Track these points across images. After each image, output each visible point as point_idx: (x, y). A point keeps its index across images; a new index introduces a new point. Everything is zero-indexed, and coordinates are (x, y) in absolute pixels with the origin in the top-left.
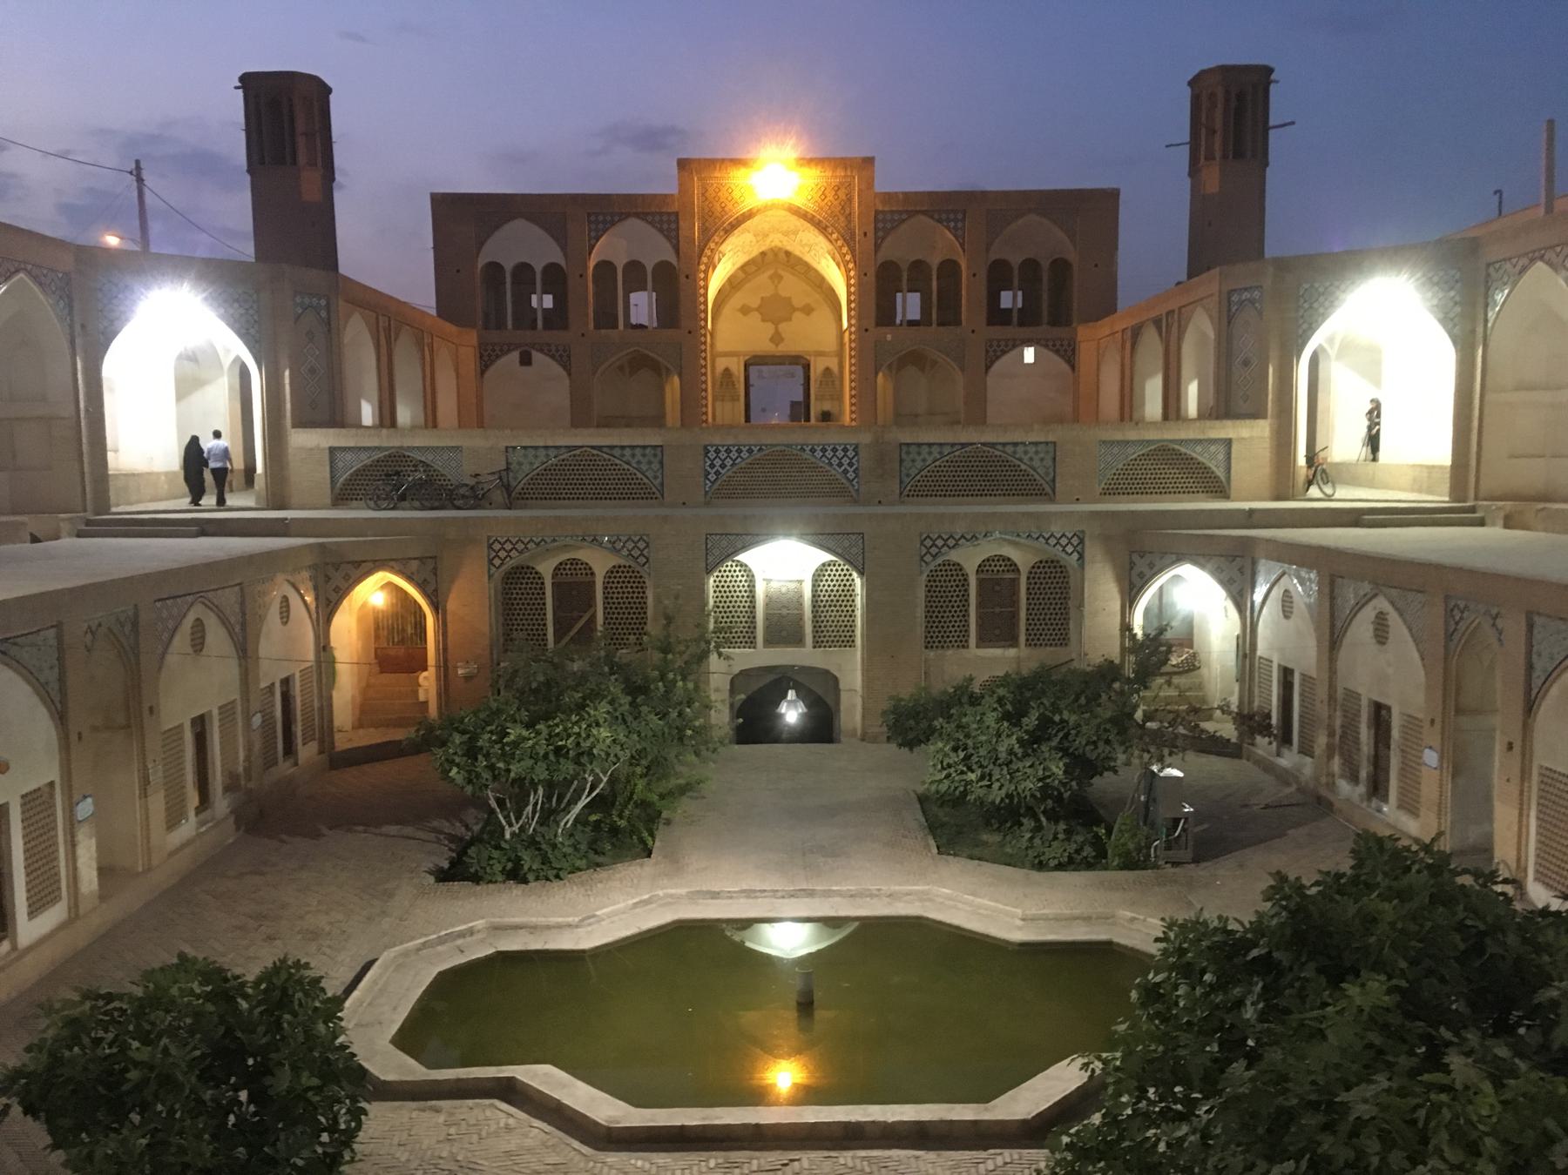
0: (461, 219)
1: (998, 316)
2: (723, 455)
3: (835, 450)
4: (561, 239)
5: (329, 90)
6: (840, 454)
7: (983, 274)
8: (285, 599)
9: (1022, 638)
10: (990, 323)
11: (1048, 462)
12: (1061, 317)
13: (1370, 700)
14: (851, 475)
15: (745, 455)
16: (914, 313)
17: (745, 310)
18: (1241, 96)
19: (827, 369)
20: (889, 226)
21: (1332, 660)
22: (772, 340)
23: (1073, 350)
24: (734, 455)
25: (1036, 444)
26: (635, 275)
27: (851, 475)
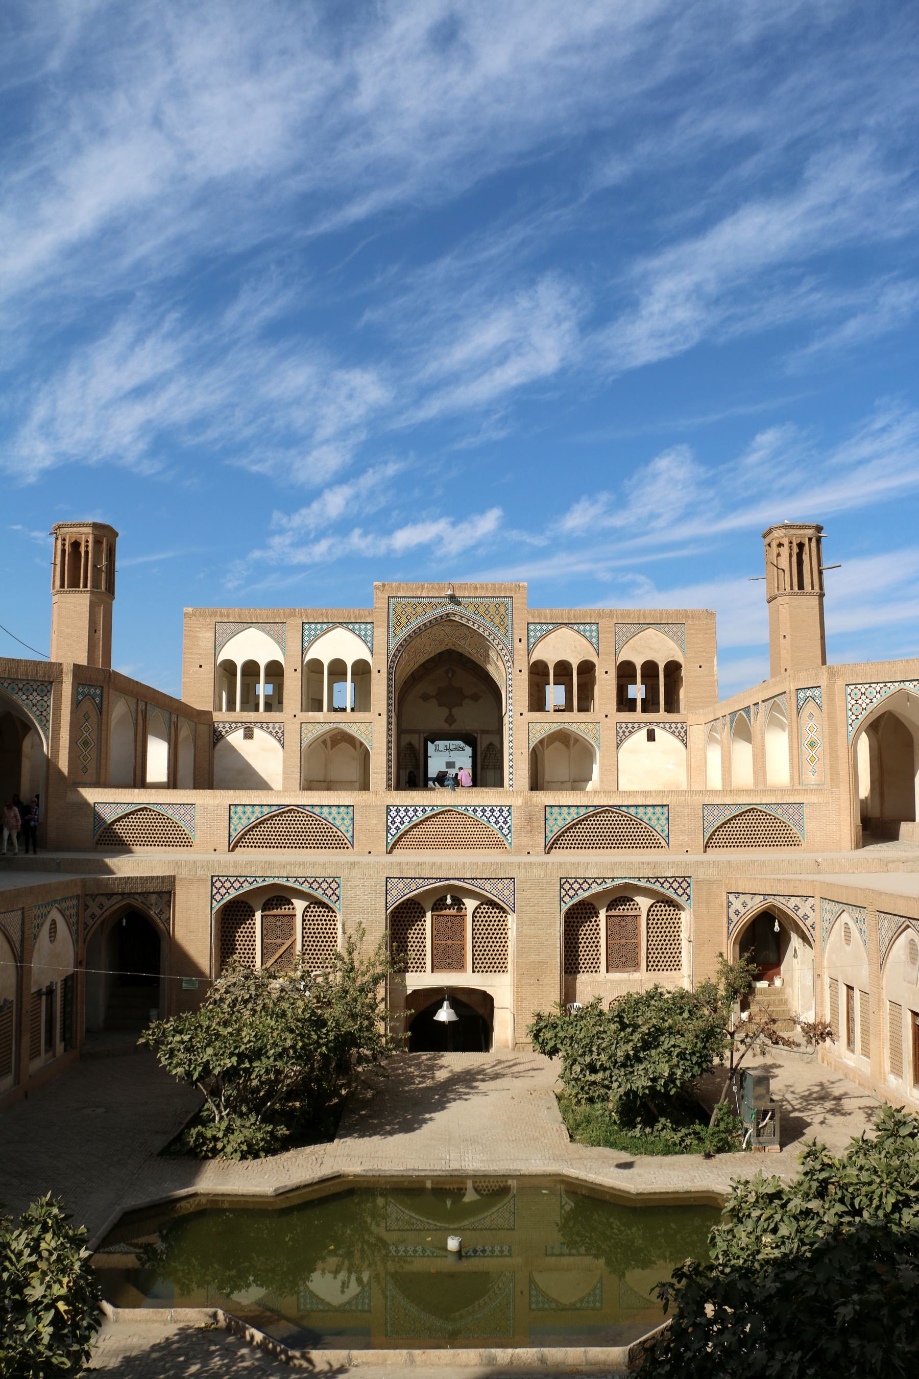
3: (492, 811)
4: (281, 642)
6: (497, 814)
7: (613, 673)
8: (54, 922)
10: (620, 709)
12: (672, 705)
13: (466, 971)
14: (505, 831)
15: (420, 814)
16: (562, 701)
17: (425, 697)
18: (801, 546)
20: (539, 634)
21: (879, 978)
22: (446, 721)
23: (685, 732)
27: (505, 831)
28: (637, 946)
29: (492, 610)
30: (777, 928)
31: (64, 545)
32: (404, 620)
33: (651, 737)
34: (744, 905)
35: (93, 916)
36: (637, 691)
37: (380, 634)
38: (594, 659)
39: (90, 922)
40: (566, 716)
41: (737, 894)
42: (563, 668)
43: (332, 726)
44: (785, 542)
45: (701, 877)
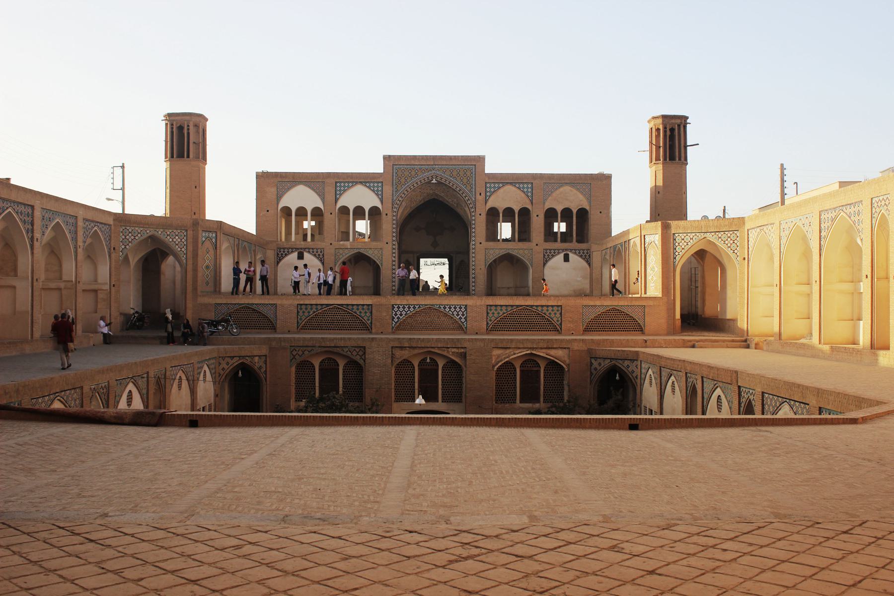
0: (271, 185)
1: (550, 235)
2: (401, 309)
3: (455, 308)
5: (207, 120)
7: (542, 216)
9: (542, 399)
10: (546, 241)
11: (558, 315)
14: (463, 320)
15: (412, 309)
18: (672, 130)
19: (462, 261)
20: (492, 190)
24: (406, 309)
25: (552, 306)
26: (359, 212)
27: (463, 320)
28: (539, 388)
29: (462, 173)
30: (617, 378)
31: (172, 128)
32: (403, 180)
33: (566, 259)
34: (600, 364)
35: (223, 369)
36: (560, 227)
37: (388, 190)
38: (529, 207)
39: (222, 372)
40: (511, 245)
41: (596, 358)
42: (509, 214)
43: (356, 251)
44: (661, 127)
45: (576, 348)
